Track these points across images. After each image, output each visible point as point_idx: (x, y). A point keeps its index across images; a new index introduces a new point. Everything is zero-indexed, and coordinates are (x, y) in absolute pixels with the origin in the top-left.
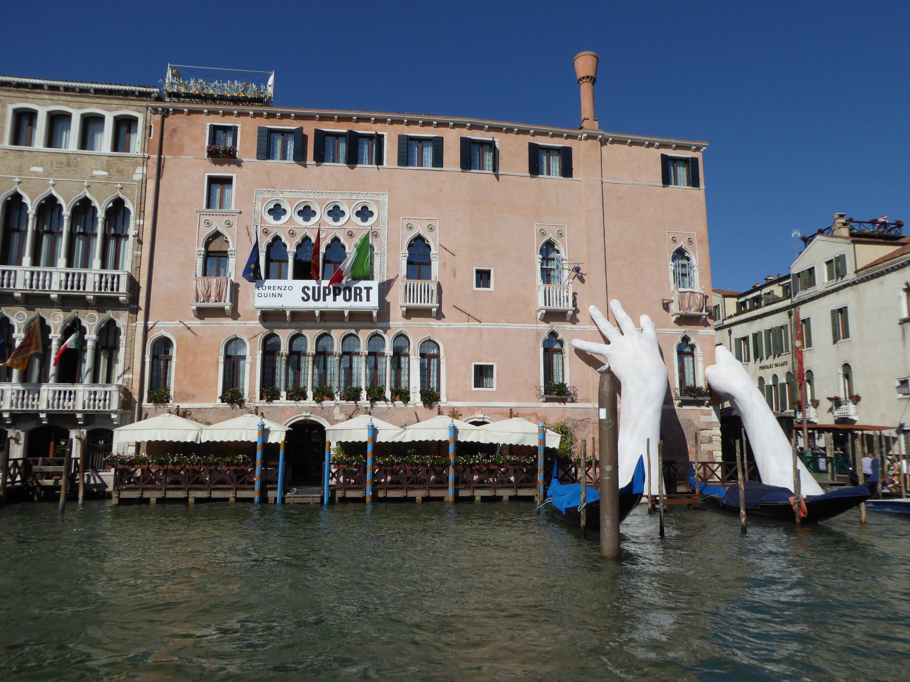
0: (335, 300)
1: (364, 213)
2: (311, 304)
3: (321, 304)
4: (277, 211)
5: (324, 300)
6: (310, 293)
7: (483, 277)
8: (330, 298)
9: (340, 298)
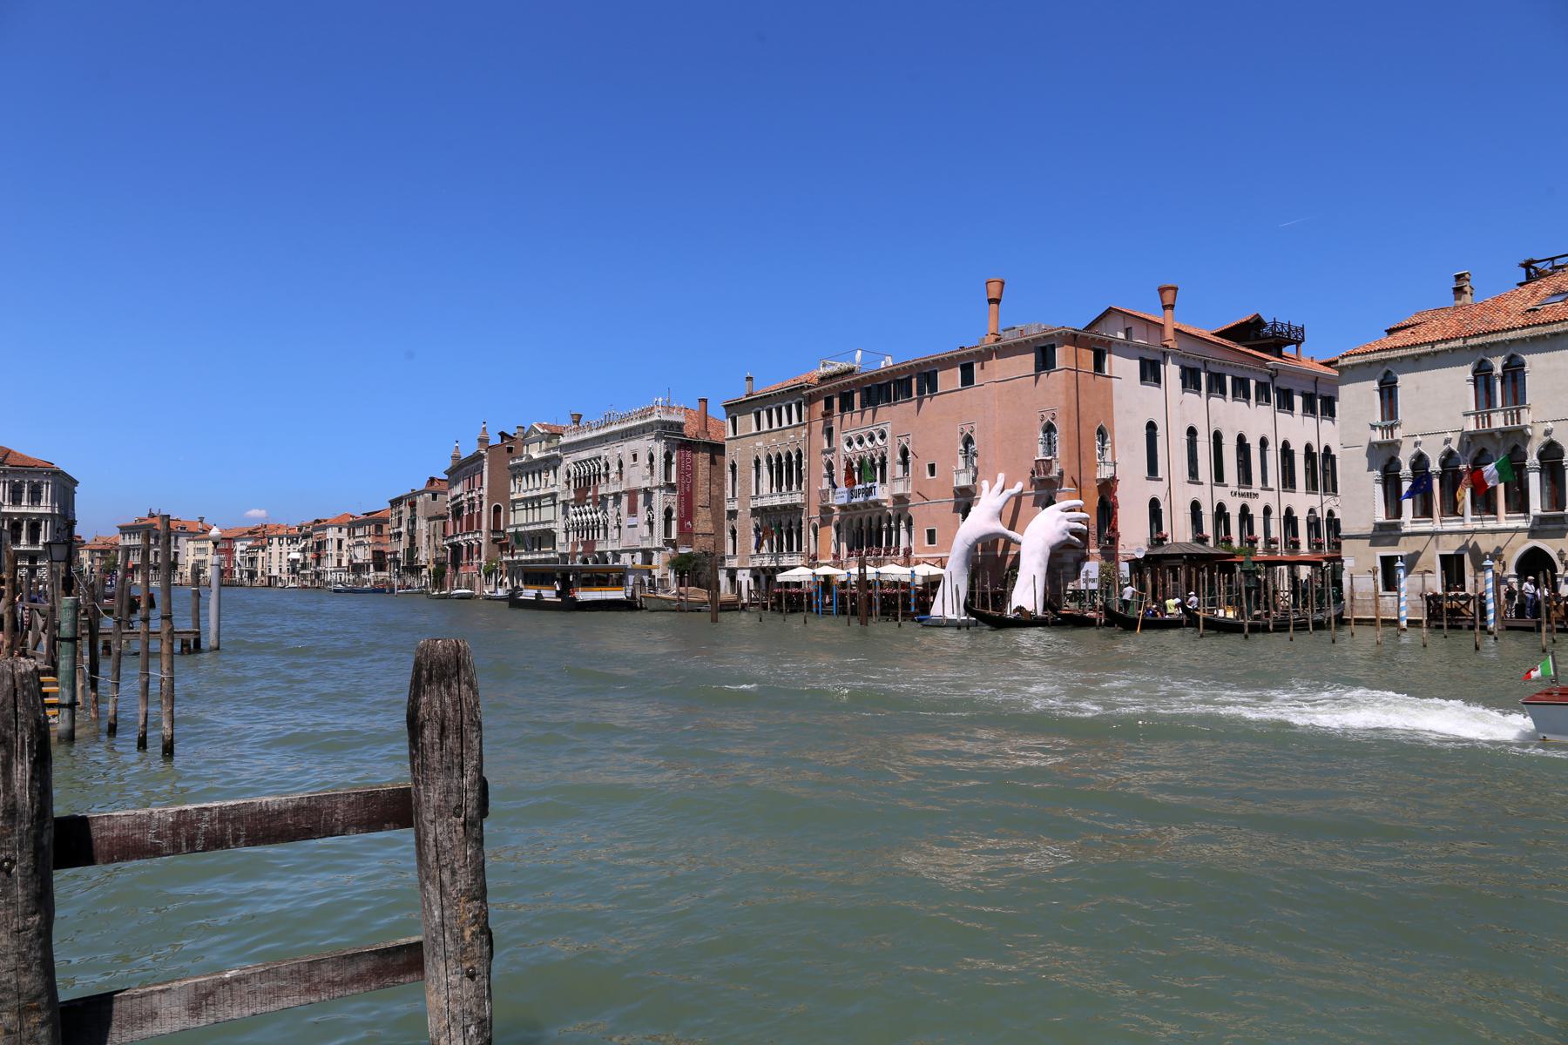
1: (883, 436)
7: (932, 468)
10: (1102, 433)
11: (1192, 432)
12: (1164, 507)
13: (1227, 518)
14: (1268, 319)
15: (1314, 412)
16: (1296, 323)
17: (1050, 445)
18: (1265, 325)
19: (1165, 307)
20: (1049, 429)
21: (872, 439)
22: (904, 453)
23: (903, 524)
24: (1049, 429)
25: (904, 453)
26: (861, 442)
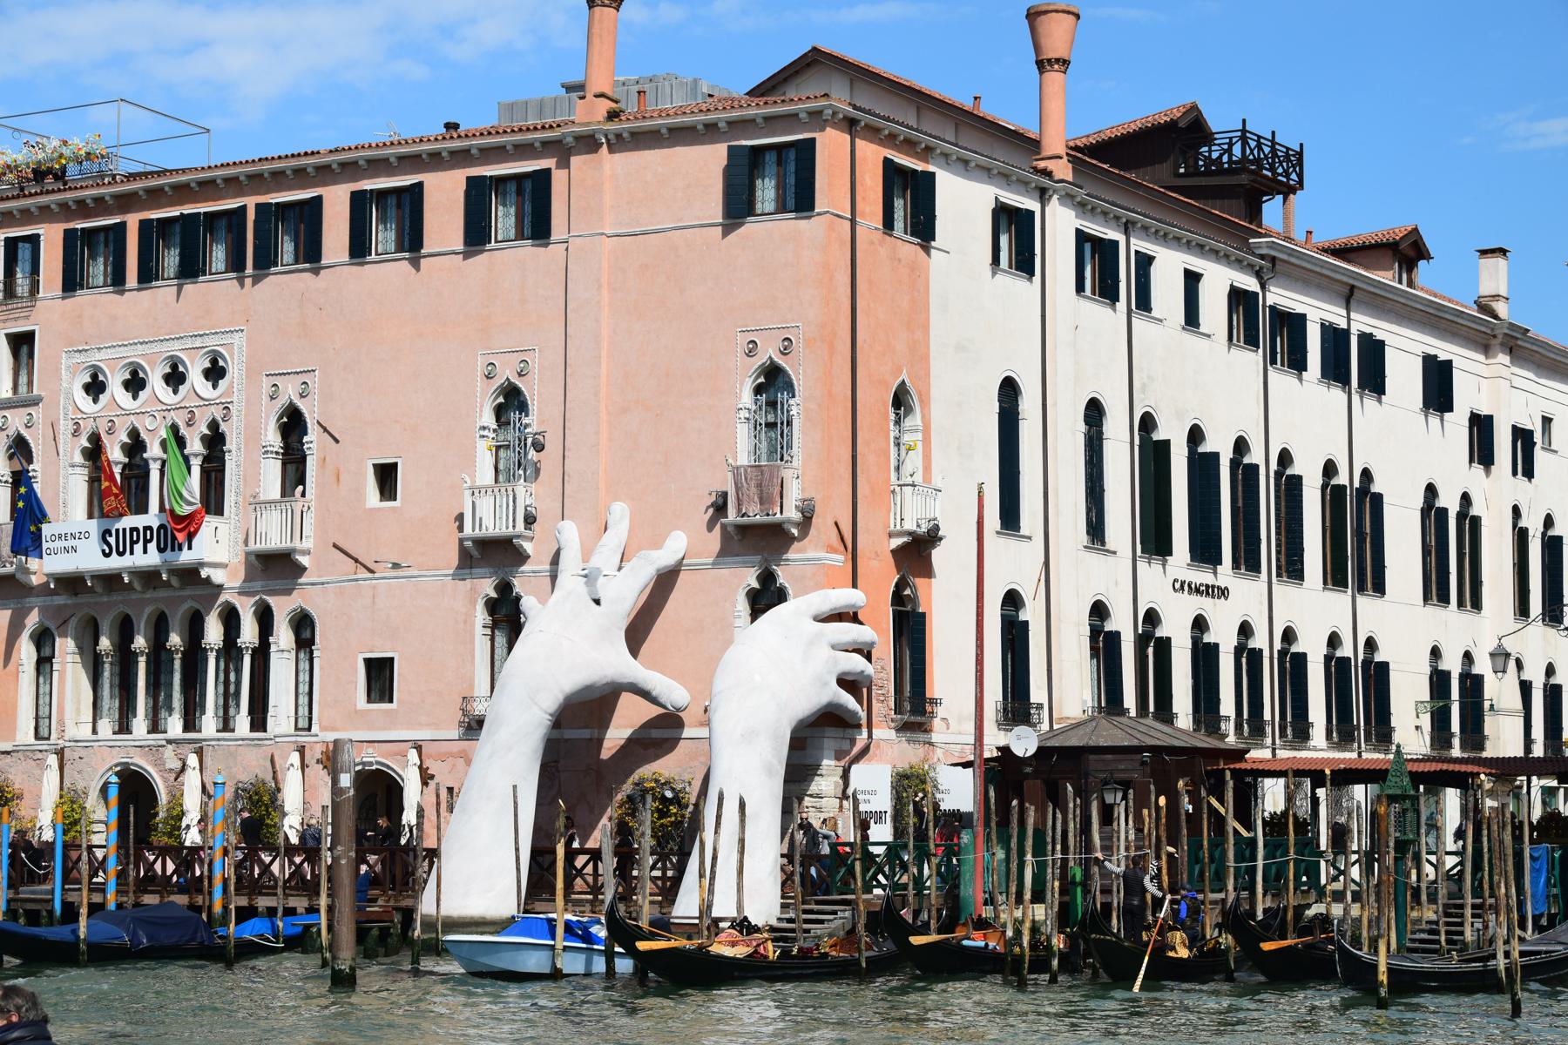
0: (145, 551)
1: (215, 373)
2: (115, 562)
3: (126, 561)
4: (95, 387)
5: (132, 553)
6: (112, 540)
7: (387, 476)
8: (139, 547)
9: (152, 546)
10: (901, 401)
11: (1094, 412)
12: (1032, 614)
13: (1164, 646)
14: (1220, 121)
15: (1344, 381)
16: (1288, 140)
17: (773, 426)
18: (1207, 137)
19: (1042, 65)
20: (773, 381)
21: (175, 378)
22: (293, 424)
23: (283, 637)
24: (773, 381)
25: (293, 424)
26: (135, 384)
